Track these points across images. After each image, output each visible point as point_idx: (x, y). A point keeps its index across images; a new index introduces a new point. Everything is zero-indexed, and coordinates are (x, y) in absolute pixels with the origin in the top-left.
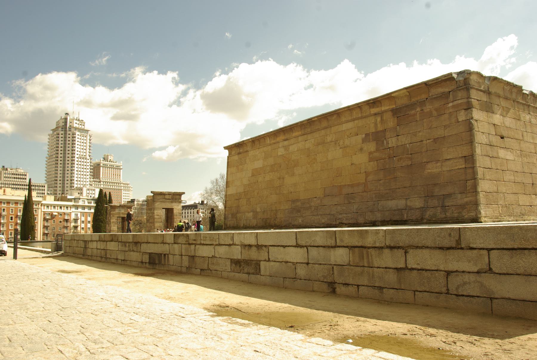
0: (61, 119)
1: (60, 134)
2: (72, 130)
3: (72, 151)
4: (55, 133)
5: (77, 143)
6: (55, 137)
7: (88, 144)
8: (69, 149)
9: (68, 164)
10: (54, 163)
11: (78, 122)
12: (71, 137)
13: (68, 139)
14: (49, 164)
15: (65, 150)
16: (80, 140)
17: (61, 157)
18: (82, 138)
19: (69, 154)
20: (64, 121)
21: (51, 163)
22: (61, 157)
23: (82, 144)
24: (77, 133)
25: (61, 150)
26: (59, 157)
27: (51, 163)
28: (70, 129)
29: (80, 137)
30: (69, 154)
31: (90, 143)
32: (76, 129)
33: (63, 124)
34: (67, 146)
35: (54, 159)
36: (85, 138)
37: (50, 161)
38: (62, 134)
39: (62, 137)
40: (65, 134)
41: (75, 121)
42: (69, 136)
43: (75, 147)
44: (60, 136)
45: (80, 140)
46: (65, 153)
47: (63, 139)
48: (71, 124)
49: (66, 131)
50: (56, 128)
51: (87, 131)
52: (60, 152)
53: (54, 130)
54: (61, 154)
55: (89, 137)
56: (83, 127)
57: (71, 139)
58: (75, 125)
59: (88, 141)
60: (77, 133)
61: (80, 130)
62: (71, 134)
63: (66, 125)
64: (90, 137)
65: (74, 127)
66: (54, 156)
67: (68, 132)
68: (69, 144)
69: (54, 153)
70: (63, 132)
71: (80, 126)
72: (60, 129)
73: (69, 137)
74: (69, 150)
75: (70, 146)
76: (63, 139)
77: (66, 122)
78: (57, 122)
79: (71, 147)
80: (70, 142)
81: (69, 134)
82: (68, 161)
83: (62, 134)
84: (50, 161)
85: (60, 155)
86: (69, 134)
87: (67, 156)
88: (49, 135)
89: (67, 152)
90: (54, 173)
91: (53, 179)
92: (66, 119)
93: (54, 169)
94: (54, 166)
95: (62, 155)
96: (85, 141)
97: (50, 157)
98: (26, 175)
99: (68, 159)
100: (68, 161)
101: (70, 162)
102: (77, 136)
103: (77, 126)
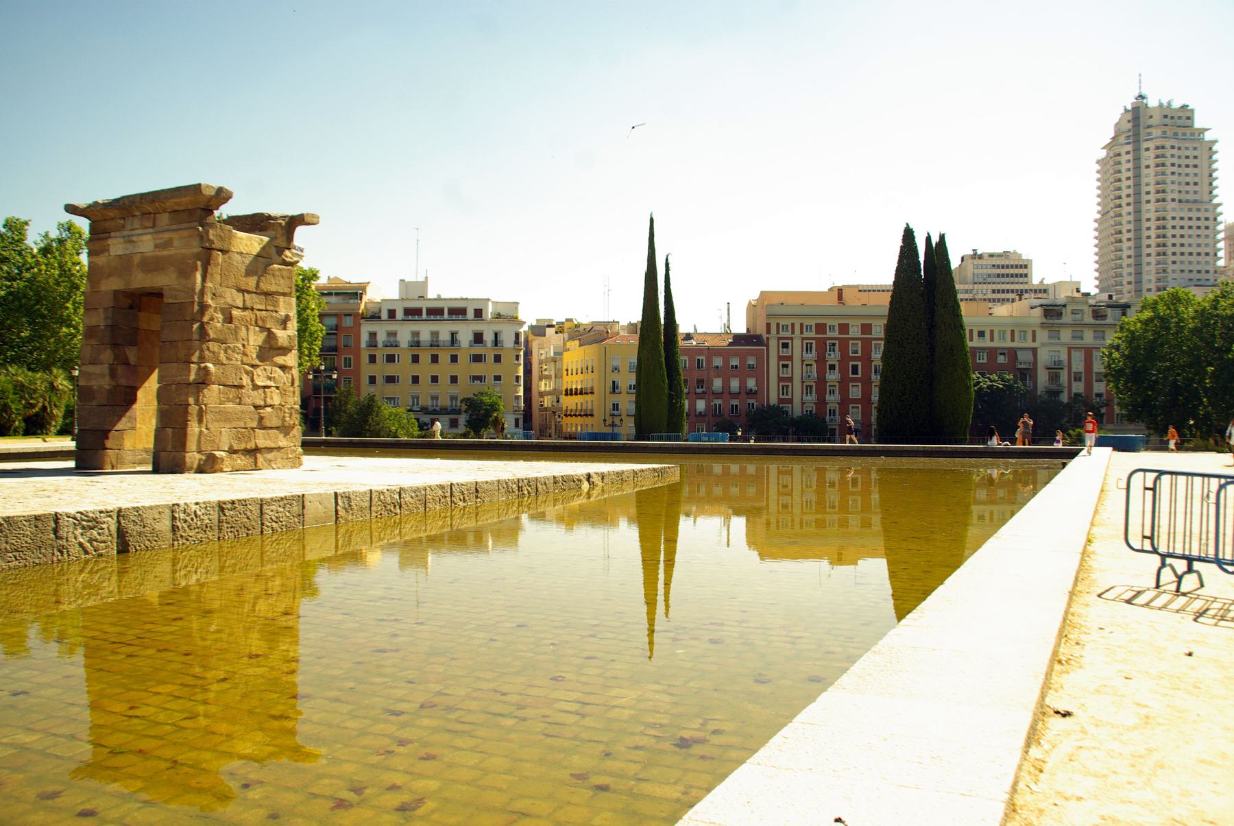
0: (1126, 111)
1: (1123, 153)
4: (1111, 154)
20: (1129, 116)
33: (1130, 125)
38: (1128, 153)
40: (1137, 150)
53: (1108, 147)
66: (1112, 214)
67: (1145, 145)
70: (1129, 148)
72: (1122, 139)
78: (1116, 125)
83: (1128, 153)
88: (1098, 162)
97: (1104, 214)
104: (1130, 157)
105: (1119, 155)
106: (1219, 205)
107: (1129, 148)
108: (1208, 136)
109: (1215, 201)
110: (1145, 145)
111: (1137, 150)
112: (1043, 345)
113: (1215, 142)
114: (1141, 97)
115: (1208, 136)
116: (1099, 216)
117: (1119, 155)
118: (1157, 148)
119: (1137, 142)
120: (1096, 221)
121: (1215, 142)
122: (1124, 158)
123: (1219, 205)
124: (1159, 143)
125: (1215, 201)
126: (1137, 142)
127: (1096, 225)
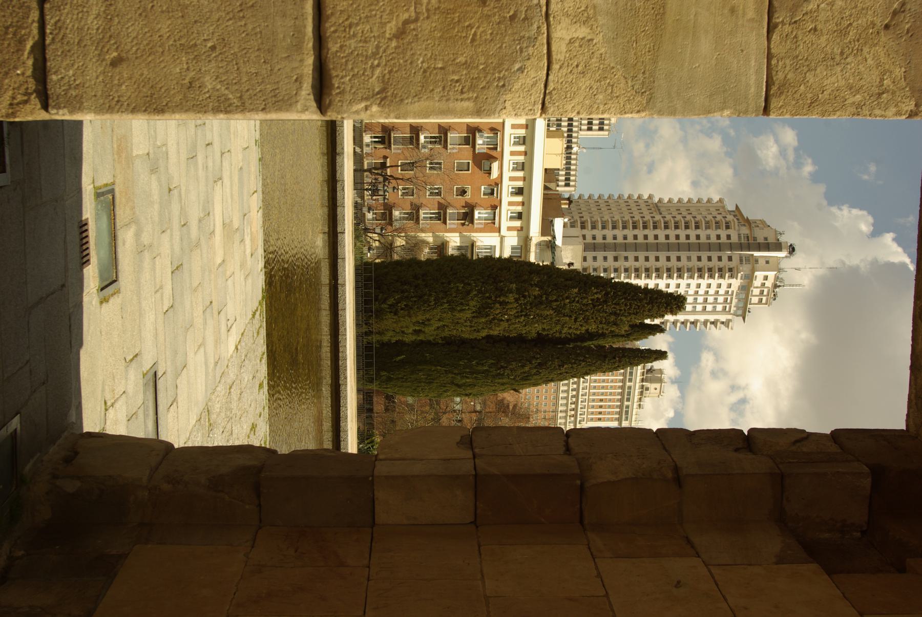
1: (729, 232)
2: (745, 269)
3: (679, 270)
4: (730, 218)
5: (704, 282)
6: (719, 218)
7: (702, 318)
8: (684, 258)
9: (636, 259)
10: (637, 217)
11: (769, 284)
12: (721, 264)
13: (715, 255)
14: (633, 205)
15: (679, 247)
16: (712, 291)
17: (656, 237)
18: (721, 299)
19: (668, 259)
20: (771, 240)
21: (634, 209)
22: (656, 237)
23: (700, 299)
24: (736, 283)
25: (677, 237)
26: (657, 232)
27: (634, 209)
28: (749, 259)
29: (722, 291)
30: (668, 259)
31: (705, 323)
32: (750, 278)
33: (760, 240)
34: (694, 255)
35: (648, 217)
36: (719, 308)
37: (643, 206)
38: (729, 237)
39: (718, 237)
40: (731, 247)
41: (771, 275)
42: (725, 259)
43: (692, 277)
44: (723, 233)
45: (712, 291)
46: (669, 247)
47: (713, 239)
48: (762, 262)
49: (741, 247)
50: (747, 220)
51: (743, 312)
52: (672, 233)
54: (667, 237)
55: (723, 318)
56: (755, 300)
57: (715, 263)
58: (759, 275)
59: (712, 318)
60: (736, 283)
61: (746, 289)
62: (732, 264)
63: (759, 247)
64: (726, 324)
65: (753, 271)
66: (658, 217)
68: (699, 259)
69: (668, 217)
71: (756, 292)
72: (745, 231)
73: (720, 259)
74: (679, 259)
75: (694, 263)
76: (713, 239)
77: (767, 247)
78: (763, 222)
79: (690, 264)
80: (704, 263)
81: (730, 259)
82: (647, 259)
83: (729, 237)
84: (643, 206)
85: (661, 233)
86: (730, 259)
87: (663, 255)
88: (721, 201)
89: (673, 255)
90: (607, 217)
91: (587, 217)
92: (778, 247)
93: (617, 217)
94: (627, 217)
95: (662, 239)
96: (709, 308)
98: (601, 129)
99: (652, 259)
100: (647, 259)
101: (641, 263)
102: (724, 282)
103: (757, 283)
107: (734, 239)
112: (502, 238)
114: (792, 250)
116: (656, 200)
120: (650, 197)
127: (646, 197)
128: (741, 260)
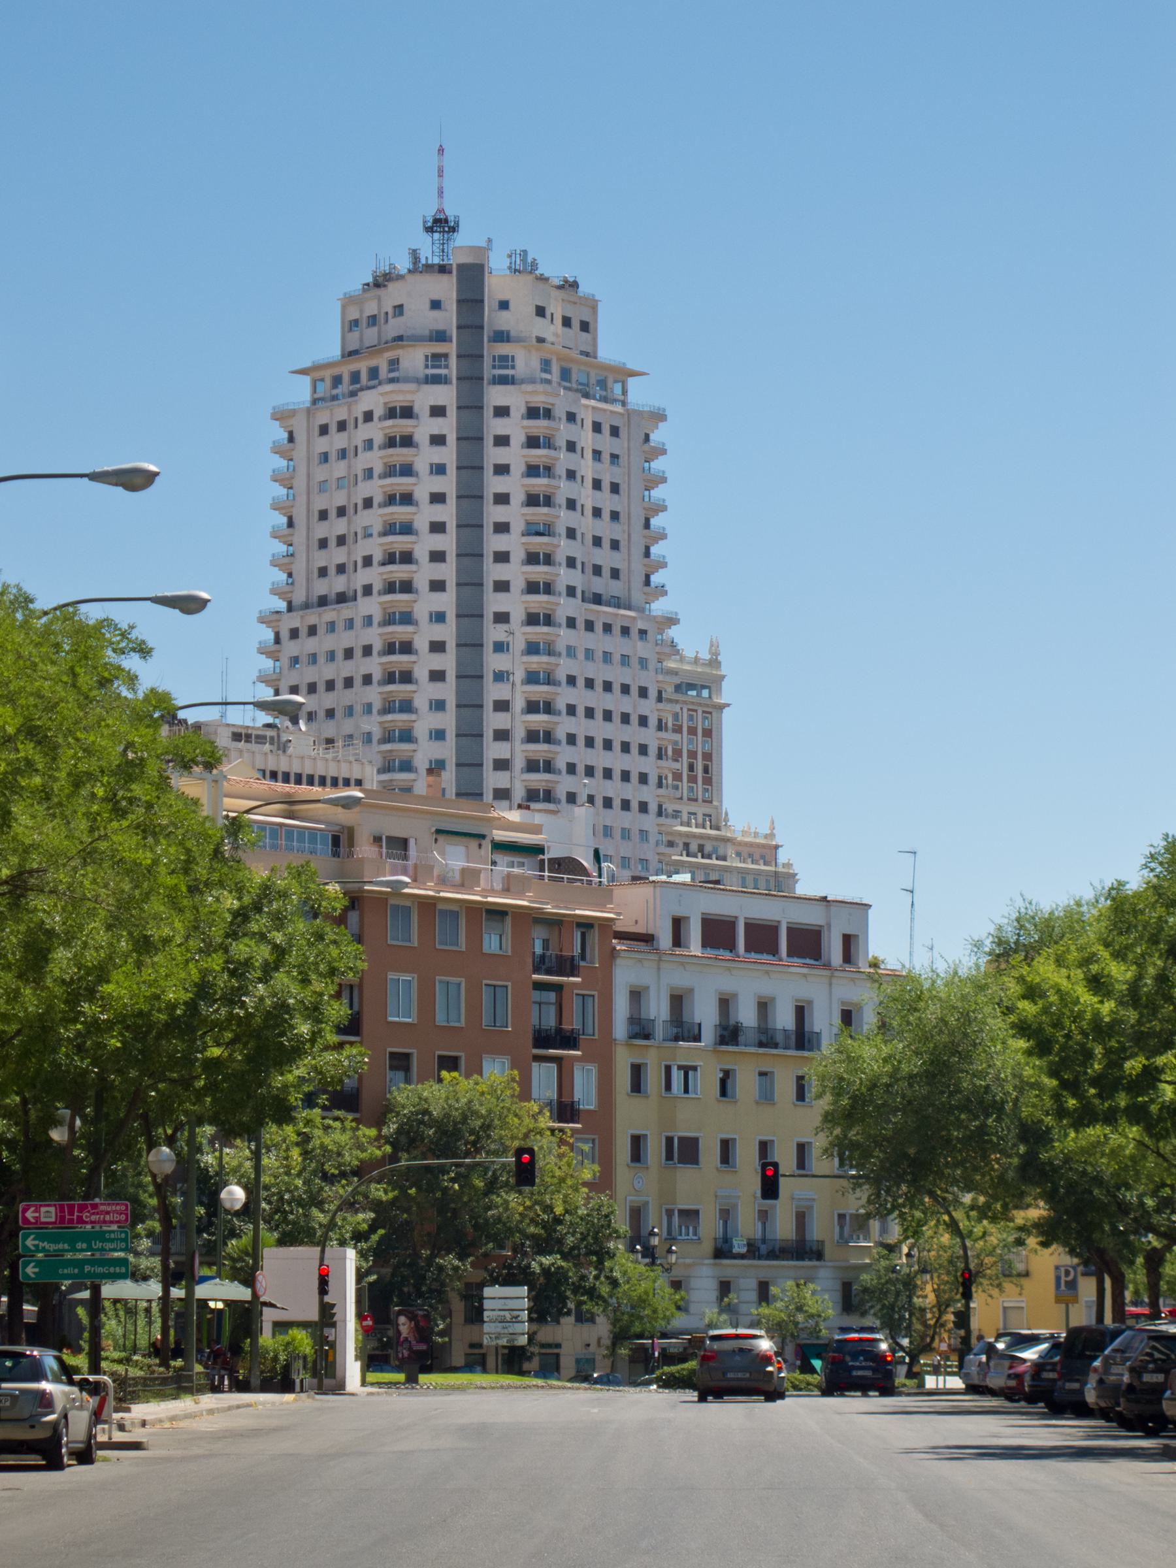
38: (438, 411)
40: (471, 406)
67: (496, 396)
81: (502, 412)
83: (438, 411)
86: (502, 412)
104: (448, 426)
105: (407, 412)
106: (672, 621)
108: (639, 395)
109: (659, 607)
110: (496, 396)
111: (471, 406)
113: (659, 416)
115: (639, 395)
117: (407, 412)
118: (532, 413)
119: (472, 382)
121: (659, 416)
122: (425, 426)
123: (672, 621)
124: (539, 400)
125: (659, 607)
126: (472, 382)
128: (504, 380)
